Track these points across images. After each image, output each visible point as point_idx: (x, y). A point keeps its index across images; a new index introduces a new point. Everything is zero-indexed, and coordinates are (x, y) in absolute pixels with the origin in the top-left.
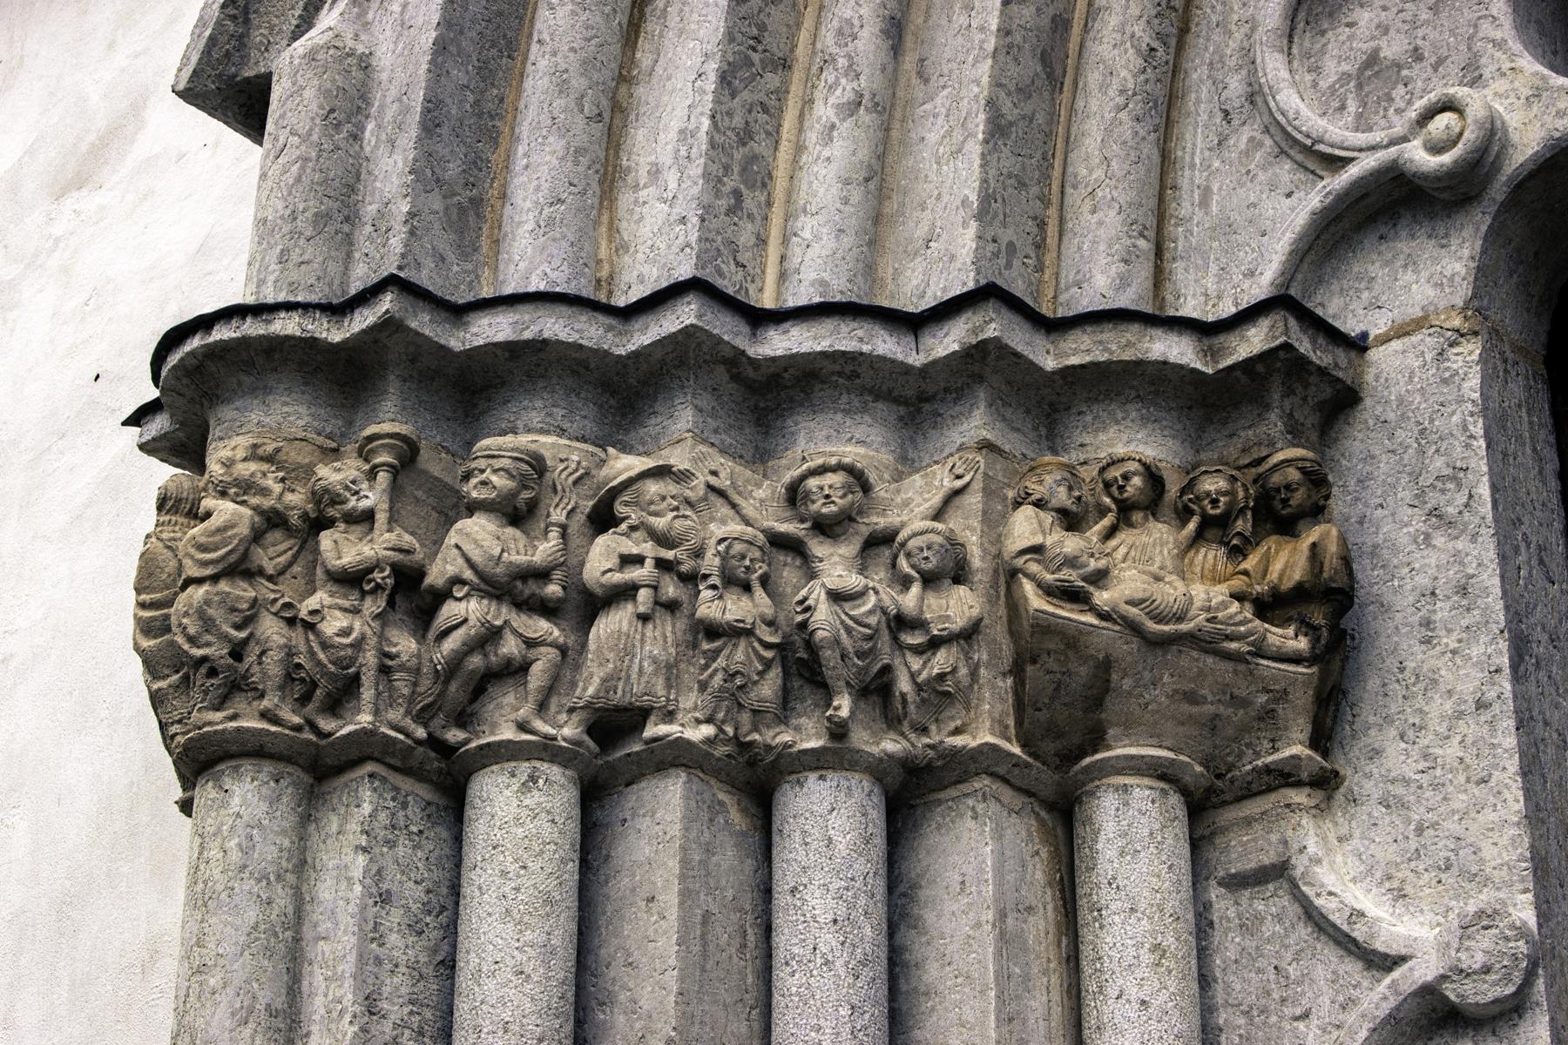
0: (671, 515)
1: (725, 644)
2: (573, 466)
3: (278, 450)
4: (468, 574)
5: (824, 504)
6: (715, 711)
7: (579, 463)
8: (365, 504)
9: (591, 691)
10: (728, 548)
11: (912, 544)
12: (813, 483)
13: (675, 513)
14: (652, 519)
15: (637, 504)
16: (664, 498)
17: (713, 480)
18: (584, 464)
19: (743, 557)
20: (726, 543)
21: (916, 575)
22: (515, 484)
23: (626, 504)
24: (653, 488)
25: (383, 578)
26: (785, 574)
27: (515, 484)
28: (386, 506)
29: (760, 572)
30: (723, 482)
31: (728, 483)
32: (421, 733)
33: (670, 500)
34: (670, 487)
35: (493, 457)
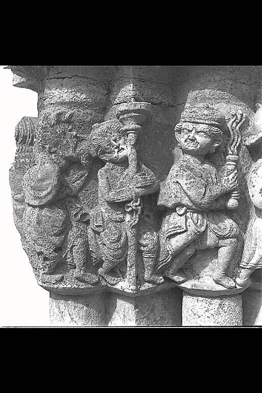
2: (239, 117)
3: (71, 115)
4: (186, 201)
7: (242, 115)
8: (122, 154)
18: (244, 114)
22: (210, 140)
25: (136, 206)
27: (210, 140)
32: (161, 279)
35: (197, 123)
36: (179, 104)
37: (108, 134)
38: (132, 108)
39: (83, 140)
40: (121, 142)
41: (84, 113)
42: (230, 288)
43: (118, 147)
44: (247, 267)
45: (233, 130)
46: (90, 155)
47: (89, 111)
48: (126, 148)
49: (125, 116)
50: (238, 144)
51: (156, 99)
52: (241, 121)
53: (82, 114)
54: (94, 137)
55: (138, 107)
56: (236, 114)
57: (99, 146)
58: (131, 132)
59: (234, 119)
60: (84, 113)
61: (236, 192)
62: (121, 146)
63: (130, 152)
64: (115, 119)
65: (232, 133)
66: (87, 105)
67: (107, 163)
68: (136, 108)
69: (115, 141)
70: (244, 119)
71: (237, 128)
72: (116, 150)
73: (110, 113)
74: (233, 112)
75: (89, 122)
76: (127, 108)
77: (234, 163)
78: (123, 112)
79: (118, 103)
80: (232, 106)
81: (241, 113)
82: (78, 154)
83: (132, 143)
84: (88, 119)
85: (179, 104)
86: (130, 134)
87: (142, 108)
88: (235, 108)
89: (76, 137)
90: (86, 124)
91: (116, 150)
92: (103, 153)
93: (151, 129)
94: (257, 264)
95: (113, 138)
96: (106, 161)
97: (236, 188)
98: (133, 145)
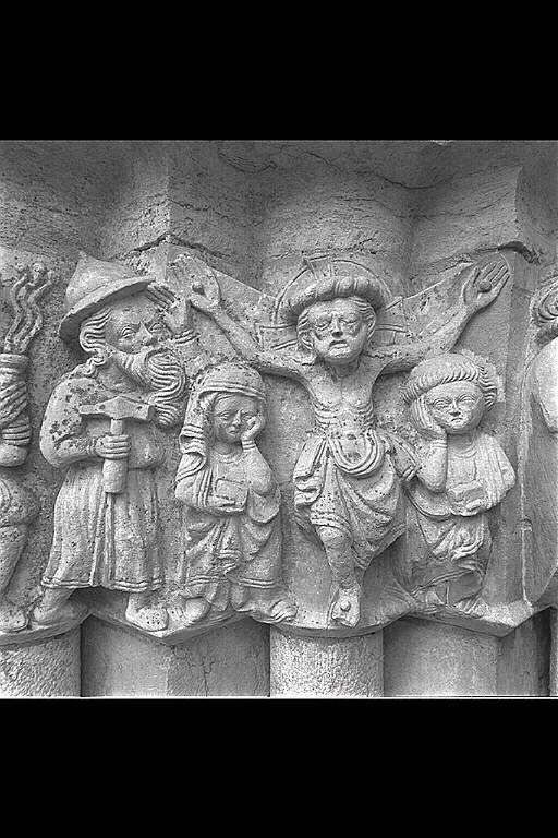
0: (145, 351)
1: (212, 526)
5: (333, 343)
6: (204, 590)
7: (44, 273)
9: (59, 574)
10: (213, 405)
11: (436, 393)
12: (317, 312)
13: (151, 348)
14: (122, 356)
15: (103, 336)
16: (137, 328)
17: (196, 299)
19: (233, 414)
20: (211, 397)
21: (438, 428)
23: (91, 336)
24: (121, 317)
26: (284, 410)
29: (255, 428)
30: (209, 302)
31: (216, 302)
33: (143, 330)
34: (147, 311)
42: (10, 631)
44: (51, 586)
45: (18, 302)
50: (33, 331)
52: (41, 282)
56: (27, 270)
59: (23, 279)
61: (11, 430)
65: (17, 308)
70: (49, 282)
71: (31, 299)
74: (21, 266)
77: (10, 370)
80: (21, 255)
81: (41, 267)
88: (29, 257)
94: (67, 579)
97: (12, 422)
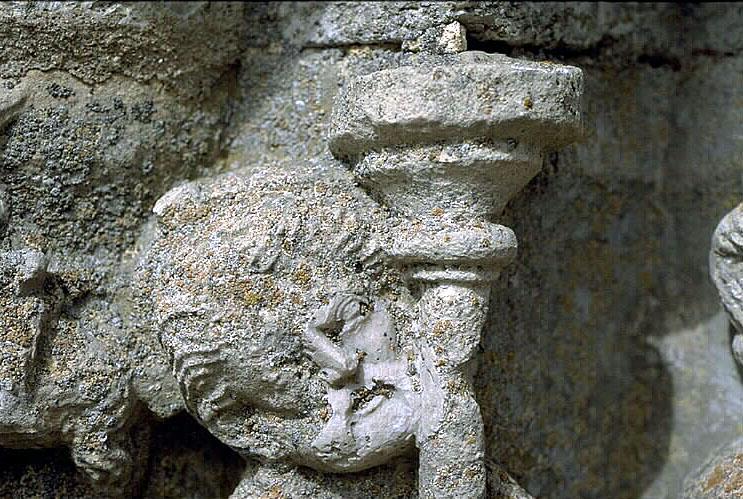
8: (379, 426)
28: (468, 448)
36: (709, 52)
37: (285, 286)
38: (469, 110)
39: (84, 297)
40: (373, 336)
41: (95, 107)
43: (350, 379)
46: (140, 410)
47: (129, 92)
48: (406, 384)
49: (414, 159)
51: (584, 19)
53: (78, 112)
54: (181, 301)
55: (510, 106)
57: (217, 368)
58: (455, 274)
60: (95, 107)
62: (372, 372)
63: (438, 415)
64: (322, 164)
66: (114, 48)
67: (264, 475)
68: (501, 111)
69: (333, 330)
72: (339, 399)
73: (274, 105)
75: (133, 169)
76: (428, 111)
78: (397, 137)
79: (332, 45)
82: (55, 411)
83: (460, 352)
84: (124, 152)
85: (709, 52)
86: (448, 293)
87: (543, 110)
89: (44, 284)
90: (107, 179)
91: (339, 399)
92: (244, 406)
93: (547, 223)
95: (323, 314)
96: (257, 461)
98: (460, 368)
